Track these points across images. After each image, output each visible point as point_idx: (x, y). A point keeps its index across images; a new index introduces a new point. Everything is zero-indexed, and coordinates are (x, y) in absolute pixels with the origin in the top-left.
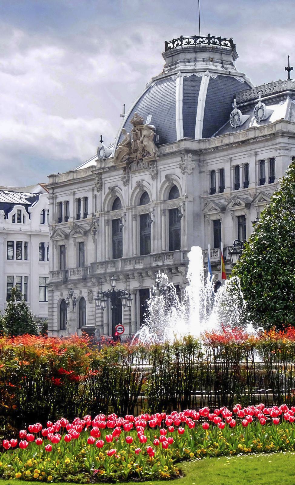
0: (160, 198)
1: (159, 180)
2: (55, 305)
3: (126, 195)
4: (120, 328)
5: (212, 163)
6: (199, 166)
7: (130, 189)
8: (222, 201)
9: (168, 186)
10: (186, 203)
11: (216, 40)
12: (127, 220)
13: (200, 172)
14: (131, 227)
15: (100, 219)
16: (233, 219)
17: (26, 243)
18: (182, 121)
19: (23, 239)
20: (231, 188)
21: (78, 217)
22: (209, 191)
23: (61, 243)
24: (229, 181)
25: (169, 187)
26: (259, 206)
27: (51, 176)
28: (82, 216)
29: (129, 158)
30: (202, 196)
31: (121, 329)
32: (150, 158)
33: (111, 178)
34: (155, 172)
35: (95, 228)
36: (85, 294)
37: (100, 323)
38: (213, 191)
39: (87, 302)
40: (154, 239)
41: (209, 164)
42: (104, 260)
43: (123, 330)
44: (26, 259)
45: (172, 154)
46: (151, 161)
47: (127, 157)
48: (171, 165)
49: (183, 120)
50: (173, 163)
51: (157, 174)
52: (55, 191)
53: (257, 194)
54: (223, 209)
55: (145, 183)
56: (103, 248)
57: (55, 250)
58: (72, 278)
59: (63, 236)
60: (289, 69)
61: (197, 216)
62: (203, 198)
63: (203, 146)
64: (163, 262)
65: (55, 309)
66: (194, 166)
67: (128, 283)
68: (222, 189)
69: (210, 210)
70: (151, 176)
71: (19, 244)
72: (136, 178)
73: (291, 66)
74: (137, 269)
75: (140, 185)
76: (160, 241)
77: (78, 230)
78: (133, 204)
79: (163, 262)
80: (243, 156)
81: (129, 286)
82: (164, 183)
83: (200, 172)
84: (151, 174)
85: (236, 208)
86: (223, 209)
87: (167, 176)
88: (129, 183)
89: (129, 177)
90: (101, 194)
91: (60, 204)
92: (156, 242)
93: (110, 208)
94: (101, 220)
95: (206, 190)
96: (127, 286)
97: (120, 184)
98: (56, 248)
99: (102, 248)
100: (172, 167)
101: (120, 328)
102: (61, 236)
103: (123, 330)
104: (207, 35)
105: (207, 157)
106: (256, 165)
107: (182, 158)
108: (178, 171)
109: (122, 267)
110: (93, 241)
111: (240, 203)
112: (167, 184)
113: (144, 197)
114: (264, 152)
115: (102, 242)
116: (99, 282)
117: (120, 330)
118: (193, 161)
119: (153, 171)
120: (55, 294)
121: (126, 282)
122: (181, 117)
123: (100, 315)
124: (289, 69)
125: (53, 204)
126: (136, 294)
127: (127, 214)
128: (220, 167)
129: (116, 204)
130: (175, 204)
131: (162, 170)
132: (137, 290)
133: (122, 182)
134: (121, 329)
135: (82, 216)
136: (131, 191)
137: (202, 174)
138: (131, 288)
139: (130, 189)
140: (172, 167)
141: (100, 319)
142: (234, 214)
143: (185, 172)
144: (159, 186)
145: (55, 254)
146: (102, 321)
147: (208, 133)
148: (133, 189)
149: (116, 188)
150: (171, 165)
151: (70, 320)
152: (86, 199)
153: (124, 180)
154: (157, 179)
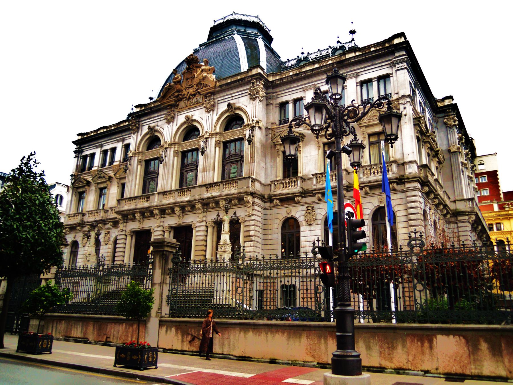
1: (215, 112)
6: (267, 98)
12: (168, 156)
14: (171, 162)
16: (319, 147)
21: (103, 165)
22: (278, 123)
28: (107, 164)
29: (178, 95)
30: (269, 127)
32: (207, 90)
33: (151, 120)
35: (126, 166)
39: (102, 243)
42: (132, 196)
46: (208, 93)
47: (176, 94)
48: (233, 95)
56: (133, 186)
57: (74, 196)
60: (353, 32)
62: (271, 129)
64: (221, 192)
72: (181, 119)
74: (178, 203)
75: (188, 119)
76: (211, 172)
79: (221, 192)
83: (268, 105)
84: (205, 107)
88: (174, 120)
90: (137, 135)
91: (86, 156)
93: (145, 148)
94: (134, 160)
99: (131, 187)
100: (234, 98)
109: (158, 201)
110: (117, 185)
115: (132, 181)
116: (124, 219)
125: (78, 157)
131: (219, 102)
135: (107, 164)
137: (271, 106)
143: (256, 97)
145: (73, 200)
148: (179, 125)
150: (233, 95)
153: (169, 118)
154: (213, 111)
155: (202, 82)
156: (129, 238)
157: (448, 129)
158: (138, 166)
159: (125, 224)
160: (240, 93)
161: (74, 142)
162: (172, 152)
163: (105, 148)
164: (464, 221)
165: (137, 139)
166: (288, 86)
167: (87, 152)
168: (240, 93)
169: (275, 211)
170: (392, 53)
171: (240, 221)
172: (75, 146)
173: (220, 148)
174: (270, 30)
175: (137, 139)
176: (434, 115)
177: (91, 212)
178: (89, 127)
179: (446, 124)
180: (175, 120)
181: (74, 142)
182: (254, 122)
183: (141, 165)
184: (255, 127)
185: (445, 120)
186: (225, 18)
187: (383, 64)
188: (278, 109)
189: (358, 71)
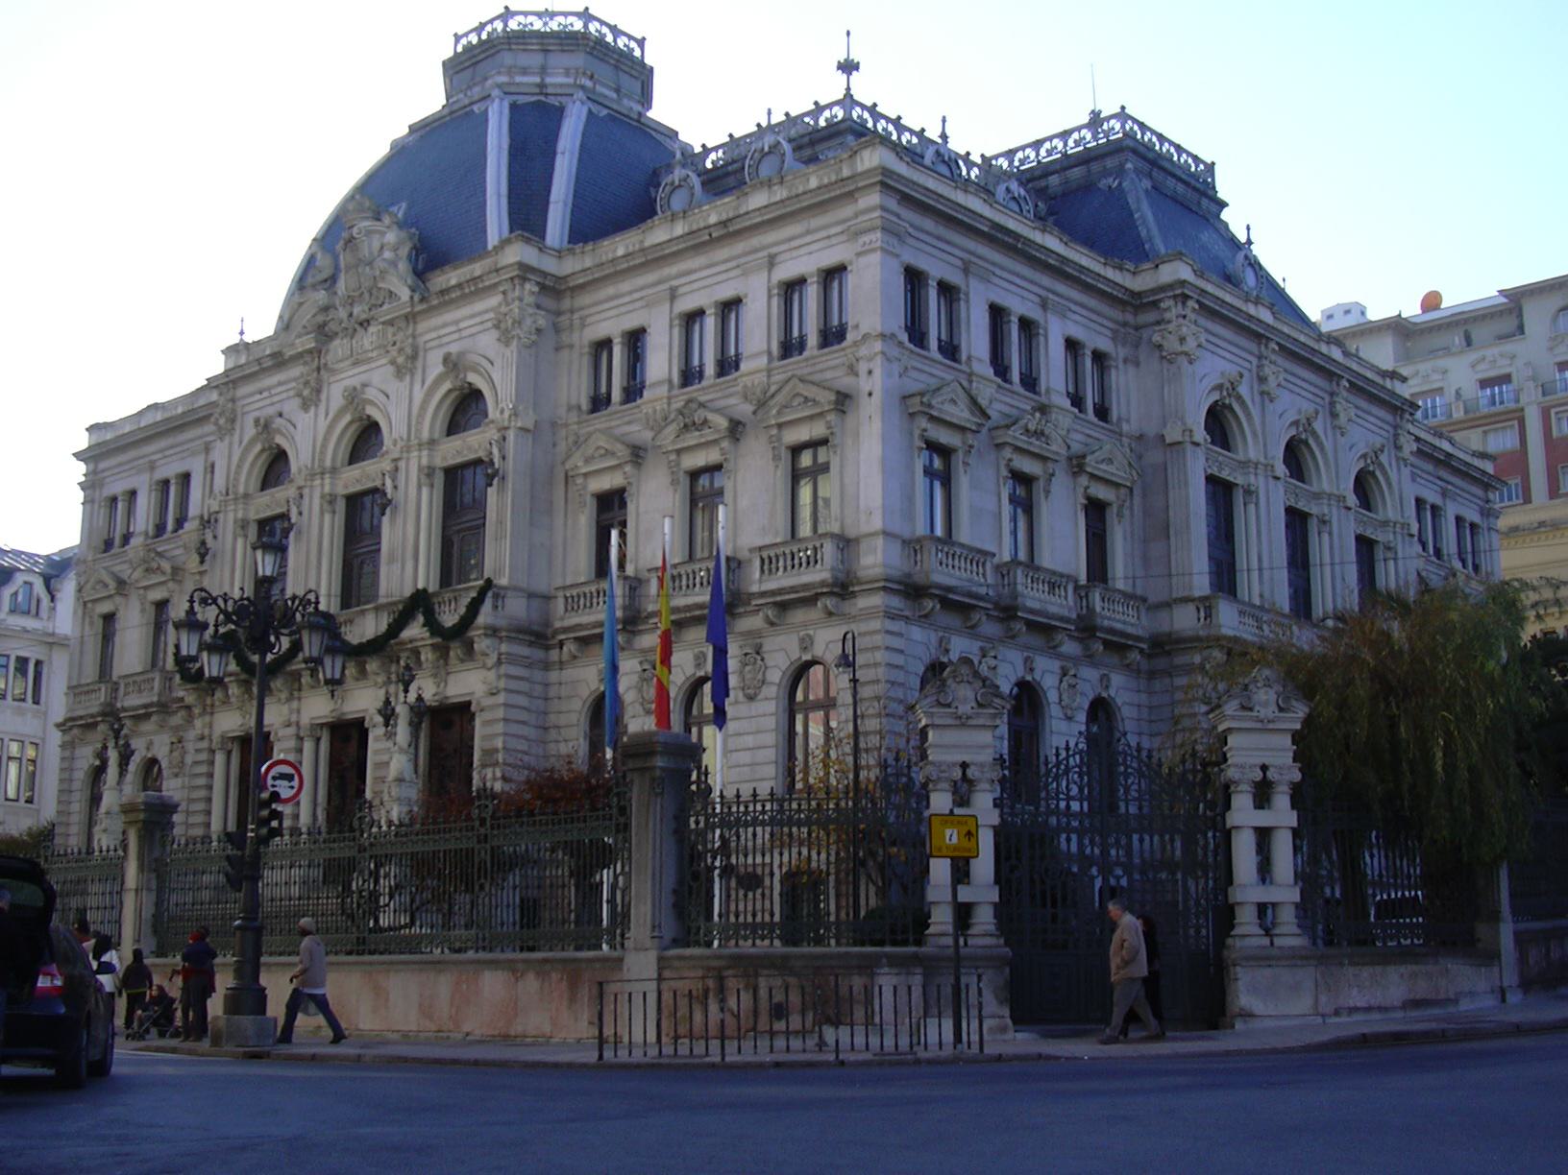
0: (419, 431)
2: (77, 785)
3: (312, 436)
4: (283, 776)
5: (597, 317)
7: (322, 416)
8: (635, 428)
9: (450, 391)
10: (511, 435)
11: (605, 30)
12: (305, 513)
13: (557, 350)
14: (315, 531)
15: (221, 516)
16: (674, 482)
17: (38, 663)
18: (504, 201)
19: (32, 654)
20: (670, 381)
21: (160, 529)
22: (585, 405)
23: (105, 608)
24: (660, 363)
25: (453, 395)
26: (780, 426)
27: (91, 429)
28: (170, 526)
31: (290, 778)
34: (409, 351)
36: (161, 751)
37: (199, 832)
38: (599, 402)
40: (392, 560)
41: (589, 320)
43: (296, 783)
44: (36, 702)
45: (472, 290)
49: (509, 197)
50: (472, 316)
51: (414, 357)
52: (102, 465)
53: (773, 389)
54: (637, 454)
55: (371, 393)
58: (126, 704)
59: (112, 585)
61: (547, 483)
63: (569, 266)
65: (76, 796)
66: (542, 322)
67: (295, 704)
68: (633, 391)
69: (588, 461)
70: (391, 369)
71: (22, 662)
73: (855, 57)
75: (354, 397)
76: (409, 565)
77: (154, 565)
78: (328, 463)
80: (724, 276)
81: (299, 711)
82: (439, 381)
84: (393, 362)
85: (692, 438)
86: (637, 454)
87: (446, 359)
89: (319, 381)
90: (231, 444)
92: (396, 567)
95: (574, 402)
96: (291, 712)
97: (291, 407)
98: (92, 623)
101: (283, 776)
102: (106, 586)
103: (296, 783)
104: (581, 9)
105: (584, 299)
106: (770, 297)
107: (504, 293)
108: (487, 342)
111: (705, 421)
112: (447, 386)
113: (366, 438)
114: (803, 251)
117: (285, 783)
118: (538, 307)
119: (401, 350)
120: (78, 752)
121: (290, 699)
122: (504, 190)
123: (201, 806)
124: (848, 67)
125: (92, 501)
126: (318, 740)
127: (306, 491)
128: (631, 322)
129: (275, 469)
130: (470, 448)
132: (322, 725)
133: (297, 401)
134: (290, 778)
136: (323, 424)
137: (565, 354)
138: (305, 720)
139: (322, 416)
140: (465, 333)
141: (200, 819)
142: (678, 464)
144: (419, 395)
146: (208, 825)
147: (586, 230)
149: (279, 420)
150: (462, 325)
151: (108, 813)
152: (186, 478)
154: (412, 375)
155: (381, 285)
156: (220, 758)
157: (1165, 364)
158: (235, 539)
159: (207, 718)
160: (478, 320)
161: (78, 456)
162: (317, 502)
163: (161, 474)
164: (1189, 670)
165: (230, 457)
166: (611, 290)
167: (118, 487)
168: (478, 320)
169: (570, 673)
170: (850, 196)
171: (473, 708)
172: (82, 467)
173: (432, 486)
174: (641, 43)
175: (230, 457)
176: (1129, 318)
177: (136, 681)
178: (121, 404)
179: (1160, 347)
180: (323, 396)
181: (78, 456)
182: (506, 414)
183: (246, 536)
184: (506, 428)
185: (1156, 338)
186: (482, 26)
187: (833, 231)
188: (586, 362)
189: (774, 250)
